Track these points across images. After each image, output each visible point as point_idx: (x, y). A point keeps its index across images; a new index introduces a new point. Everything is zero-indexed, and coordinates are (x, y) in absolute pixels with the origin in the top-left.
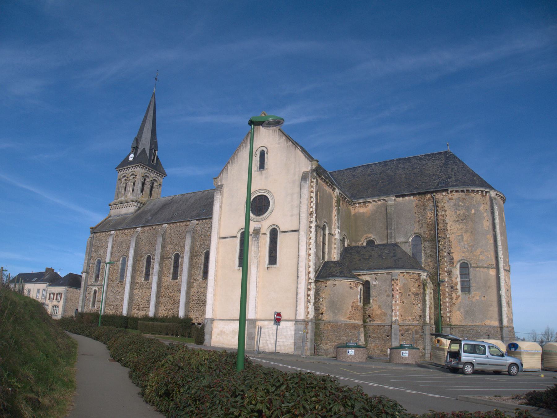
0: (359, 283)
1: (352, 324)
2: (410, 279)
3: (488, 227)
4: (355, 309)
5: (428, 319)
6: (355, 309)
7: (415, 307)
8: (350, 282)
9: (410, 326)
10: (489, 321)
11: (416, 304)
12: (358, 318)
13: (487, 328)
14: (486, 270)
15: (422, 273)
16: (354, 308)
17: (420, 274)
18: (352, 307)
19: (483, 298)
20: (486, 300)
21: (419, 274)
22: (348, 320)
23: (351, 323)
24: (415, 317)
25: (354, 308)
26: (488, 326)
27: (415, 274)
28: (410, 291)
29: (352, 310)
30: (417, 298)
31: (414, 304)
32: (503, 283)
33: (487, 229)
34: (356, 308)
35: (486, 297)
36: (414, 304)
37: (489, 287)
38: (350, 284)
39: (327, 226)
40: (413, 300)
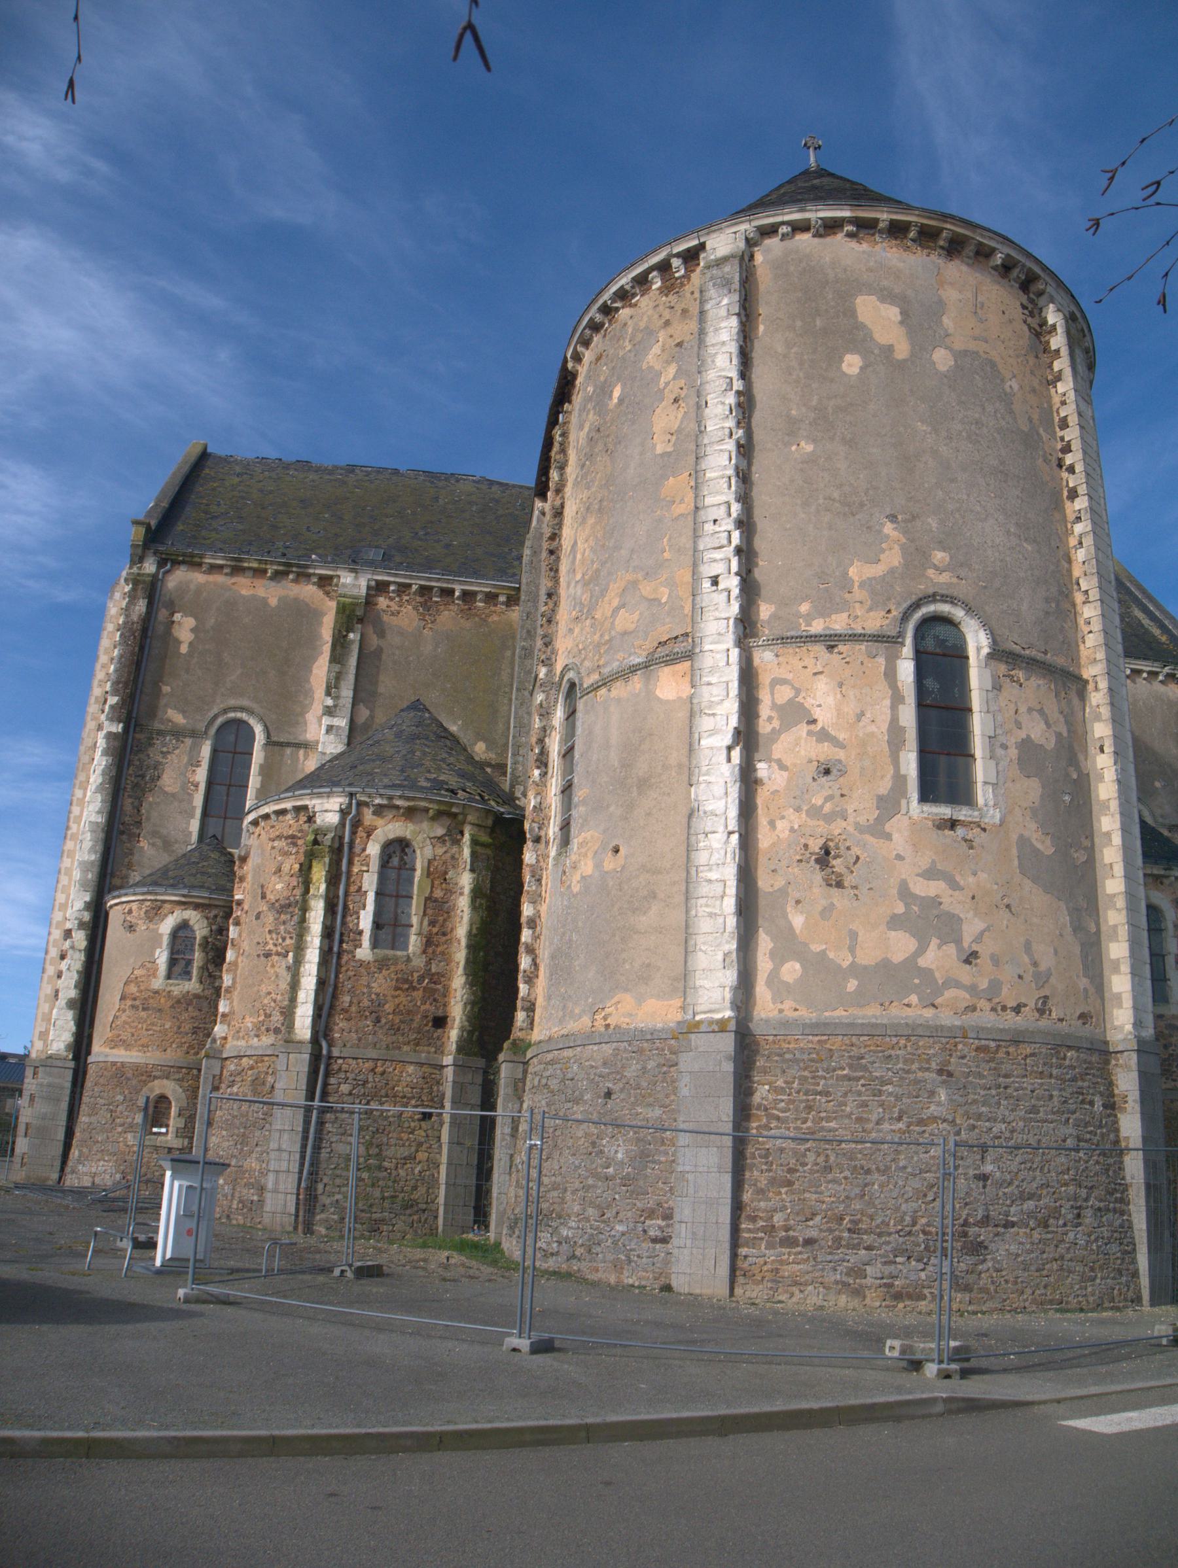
0: (164, 902)
1: (114, 1064)
2: (271, 844)
3: (679, 431)
4: (133, 1006)
5: (308, 1021)
6: (133, 1006)
7: (273, 966)
8: (128, 907)
9: (245, 1060)
10: (627, 1001)
11: (278, 954)
12: (144, 1041)
13: (608, 1049)
14: (637, 683)
15: (315, 803)
16: (129, 1002)
17: (305, 808)
18: (123, 998)
19: (610, 863)
20: (623, 867)
21: (298, 809)
22: (107, 1050)
23: (110, 1059)
24: (266, 1014)
25: (129, 1002)
26: (613, 1034)
27: (289, 817)
28: (264, 897)
29: (124, 1011)
30: (284, 923)
31: (268, 955)
32: (713, 732)
33: (670, 449)
34: (137, 1003)
35: (622, 851)
36: (268, 955)
37: (644, 784)
38: (130, 912)
39: (252, 721)
40: (268, 937)
